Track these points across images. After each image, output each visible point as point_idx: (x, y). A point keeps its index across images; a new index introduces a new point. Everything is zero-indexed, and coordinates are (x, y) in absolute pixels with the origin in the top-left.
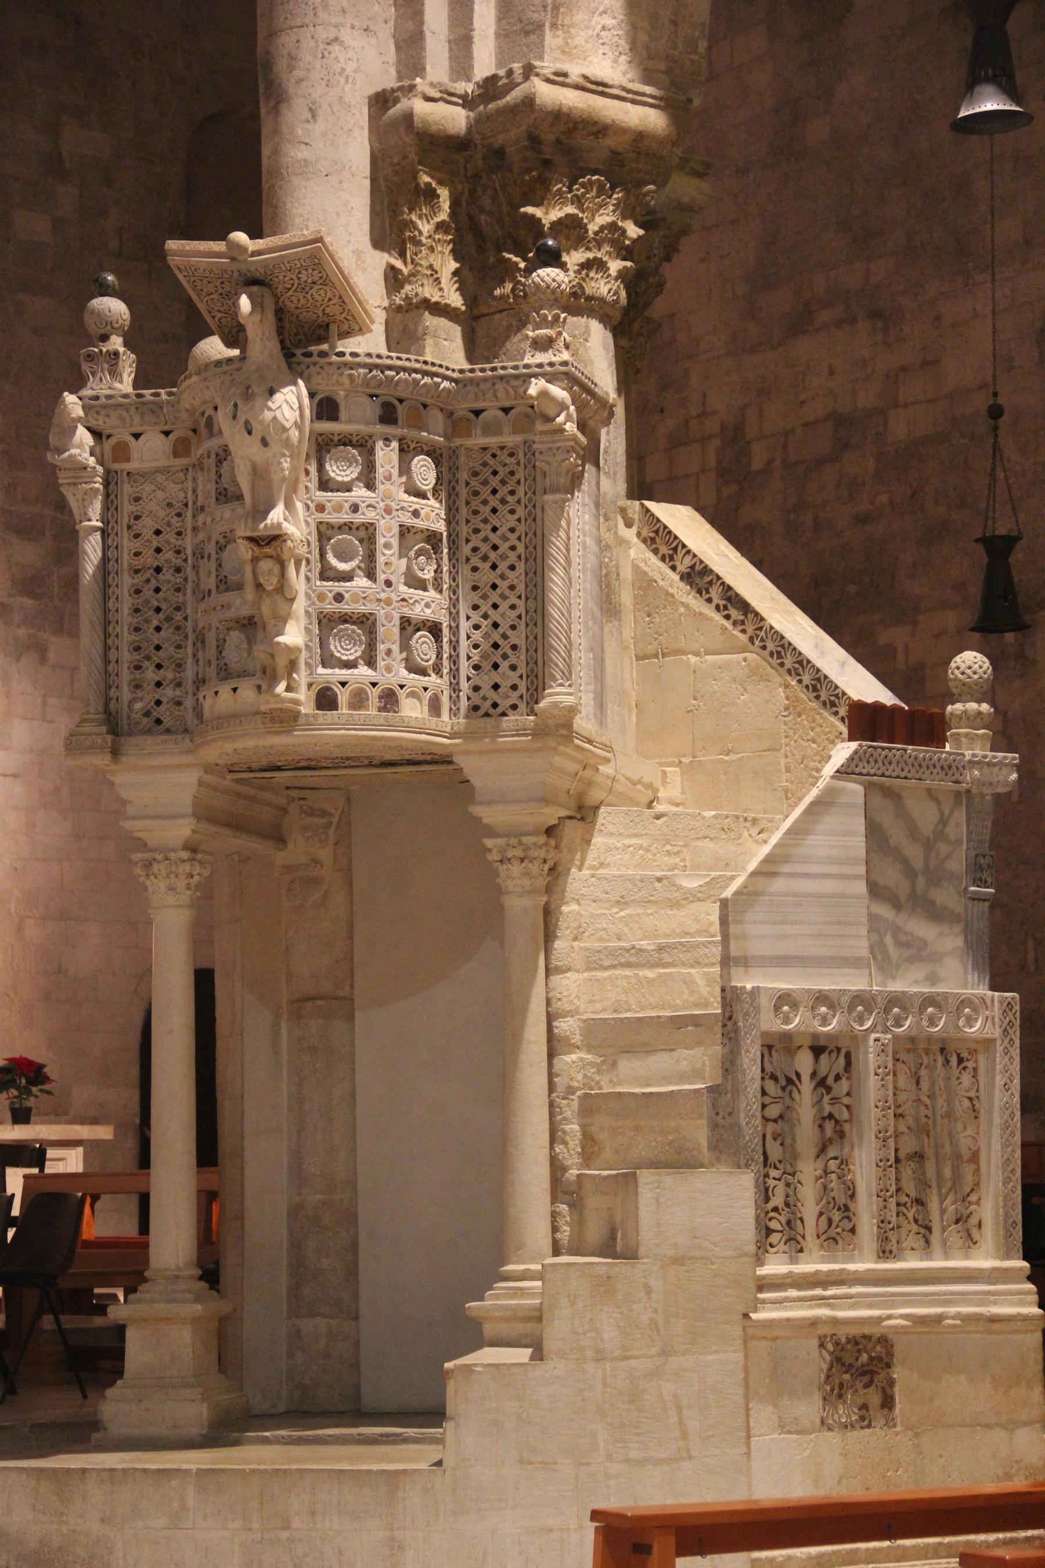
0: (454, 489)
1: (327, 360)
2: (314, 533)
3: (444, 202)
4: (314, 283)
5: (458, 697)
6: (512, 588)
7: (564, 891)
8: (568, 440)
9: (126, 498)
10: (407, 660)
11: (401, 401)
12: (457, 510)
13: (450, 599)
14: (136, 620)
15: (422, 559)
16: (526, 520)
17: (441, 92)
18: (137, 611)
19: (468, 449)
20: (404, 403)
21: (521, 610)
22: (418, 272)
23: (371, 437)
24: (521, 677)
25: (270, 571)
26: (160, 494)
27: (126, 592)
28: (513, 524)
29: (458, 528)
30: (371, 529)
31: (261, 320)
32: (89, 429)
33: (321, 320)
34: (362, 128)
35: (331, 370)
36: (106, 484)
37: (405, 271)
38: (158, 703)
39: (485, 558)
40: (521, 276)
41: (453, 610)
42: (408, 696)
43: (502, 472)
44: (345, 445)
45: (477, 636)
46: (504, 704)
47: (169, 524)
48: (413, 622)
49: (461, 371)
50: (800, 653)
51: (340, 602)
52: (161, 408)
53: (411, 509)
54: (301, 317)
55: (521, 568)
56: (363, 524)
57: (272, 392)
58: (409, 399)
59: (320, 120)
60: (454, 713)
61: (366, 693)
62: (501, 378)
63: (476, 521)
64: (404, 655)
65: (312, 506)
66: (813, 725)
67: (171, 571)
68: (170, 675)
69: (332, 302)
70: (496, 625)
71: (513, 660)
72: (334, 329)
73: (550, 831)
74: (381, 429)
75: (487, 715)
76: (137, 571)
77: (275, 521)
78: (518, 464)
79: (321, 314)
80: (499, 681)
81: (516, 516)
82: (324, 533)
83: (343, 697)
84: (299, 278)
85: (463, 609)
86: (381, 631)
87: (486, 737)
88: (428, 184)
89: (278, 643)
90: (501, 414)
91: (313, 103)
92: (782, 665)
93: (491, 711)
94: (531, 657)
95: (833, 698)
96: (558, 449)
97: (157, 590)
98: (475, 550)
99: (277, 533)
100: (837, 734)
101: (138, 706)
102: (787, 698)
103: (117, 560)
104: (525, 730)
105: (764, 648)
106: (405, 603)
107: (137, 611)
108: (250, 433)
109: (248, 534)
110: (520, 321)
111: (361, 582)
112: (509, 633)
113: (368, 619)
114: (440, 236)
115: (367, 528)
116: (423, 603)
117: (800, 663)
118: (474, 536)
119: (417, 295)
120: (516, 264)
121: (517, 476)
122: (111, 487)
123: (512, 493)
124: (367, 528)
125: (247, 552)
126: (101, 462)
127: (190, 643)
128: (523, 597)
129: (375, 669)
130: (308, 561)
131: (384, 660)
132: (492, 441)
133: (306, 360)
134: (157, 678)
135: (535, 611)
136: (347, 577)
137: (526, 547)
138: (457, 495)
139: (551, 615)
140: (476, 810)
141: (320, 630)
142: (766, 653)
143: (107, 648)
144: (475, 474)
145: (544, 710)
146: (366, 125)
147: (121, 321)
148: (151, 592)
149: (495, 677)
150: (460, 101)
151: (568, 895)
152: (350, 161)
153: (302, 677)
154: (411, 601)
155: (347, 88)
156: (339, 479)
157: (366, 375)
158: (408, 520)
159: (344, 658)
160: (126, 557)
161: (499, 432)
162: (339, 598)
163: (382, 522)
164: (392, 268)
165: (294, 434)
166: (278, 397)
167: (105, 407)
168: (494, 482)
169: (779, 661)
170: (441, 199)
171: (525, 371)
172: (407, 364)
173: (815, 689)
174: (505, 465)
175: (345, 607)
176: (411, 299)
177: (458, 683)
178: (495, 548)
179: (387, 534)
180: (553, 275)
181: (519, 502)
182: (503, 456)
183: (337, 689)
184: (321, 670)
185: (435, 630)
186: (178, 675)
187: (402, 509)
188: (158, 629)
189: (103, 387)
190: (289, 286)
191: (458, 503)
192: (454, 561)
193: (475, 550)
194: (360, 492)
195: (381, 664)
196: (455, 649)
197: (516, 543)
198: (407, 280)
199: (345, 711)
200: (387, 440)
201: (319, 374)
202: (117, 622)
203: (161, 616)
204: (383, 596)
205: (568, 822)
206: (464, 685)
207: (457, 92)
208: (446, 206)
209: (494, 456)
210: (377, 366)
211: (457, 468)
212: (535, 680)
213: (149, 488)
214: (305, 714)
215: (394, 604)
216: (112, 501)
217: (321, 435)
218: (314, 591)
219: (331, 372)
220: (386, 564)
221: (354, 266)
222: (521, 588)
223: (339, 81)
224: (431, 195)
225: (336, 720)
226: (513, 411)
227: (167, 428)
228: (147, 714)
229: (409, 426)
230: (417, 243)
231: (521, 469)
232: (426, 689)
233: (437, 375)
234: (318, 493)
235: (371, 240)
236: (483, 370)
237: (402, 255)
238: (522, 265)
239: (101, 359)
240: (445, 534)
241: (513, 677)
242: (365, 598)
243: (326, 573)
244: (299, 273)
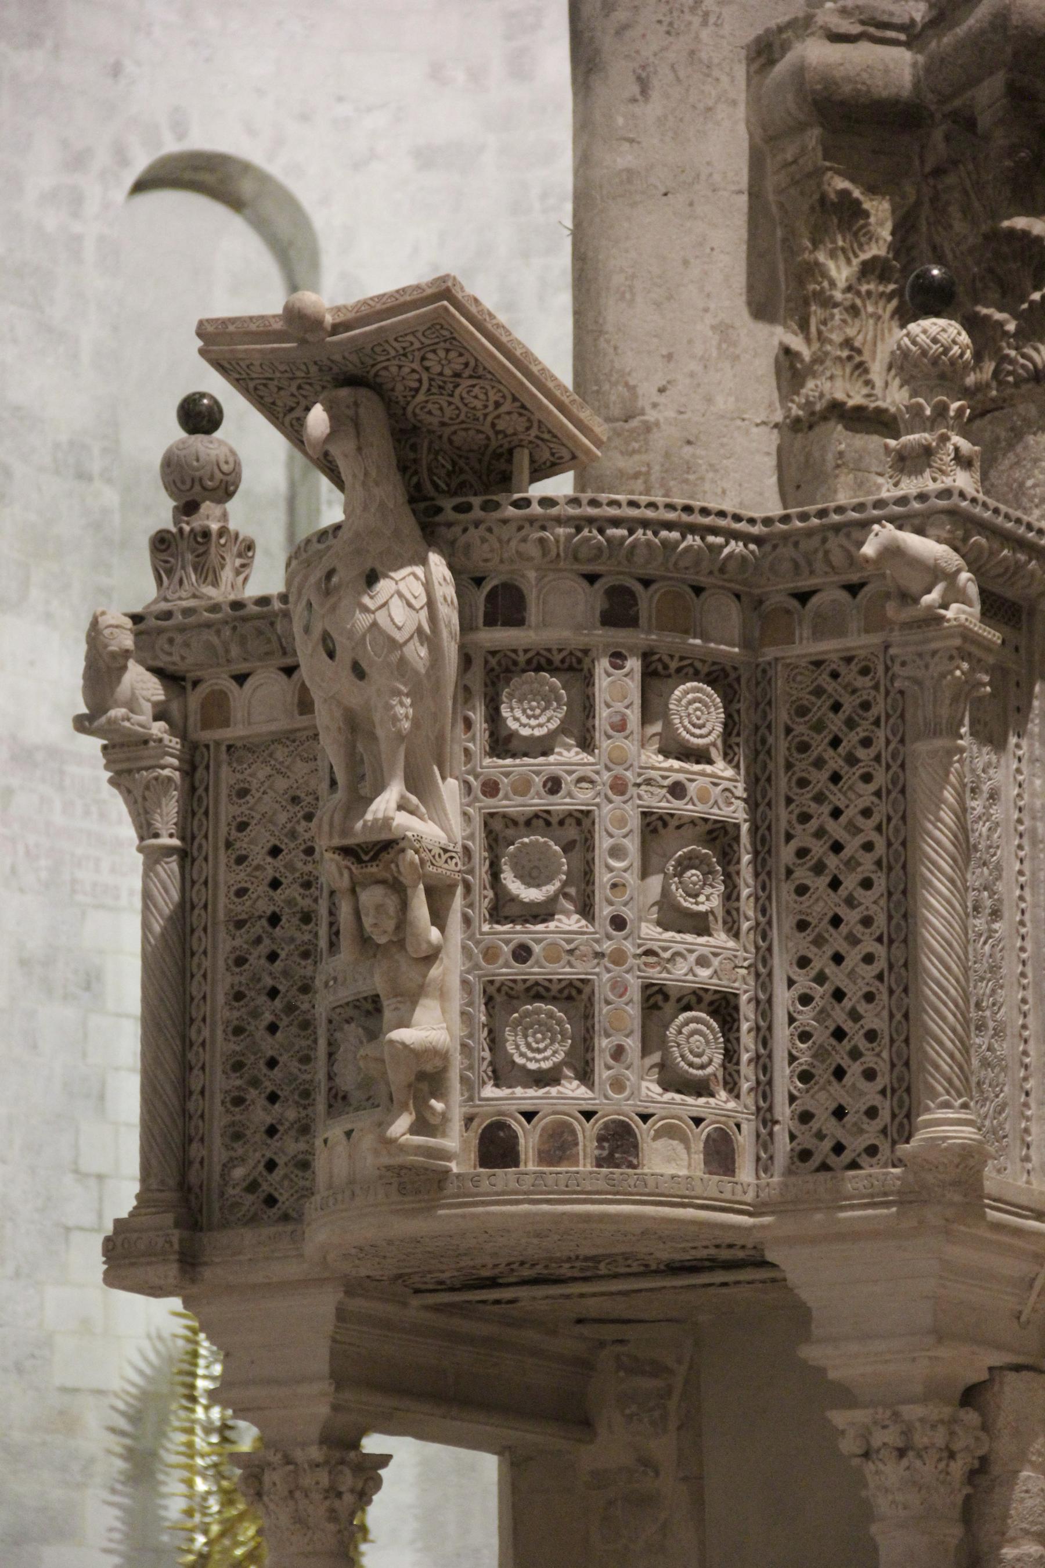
0: (764, 741)
1: (497, 515)
2: (480, 834)
3: (881, 224)
4: (457, 375)
5: (771, 1134)
7: (1006, 1516)
8: (951, 636)
9: (224, 791)
10: (662, 1066)
11: (647, 583)
12: (769, 780)
13: (757, 948)
14: (236, 1014)
15: (693, 875)
16: (889, 792)
17: (863, 23)
18: (239, 996)
19: (791, 667)
20: (654, 587)
21: (881, 964)
22: (827, 354)
23: (586, 652)
24: (883, 1092)
25: (379, 908)
26: (281, 784)
27: (221, 963)
28: (867, 801)
29: (771, 815)
30: (586, 823)
31: (359, 449)
32: (158, 672)
33: (494, 444)
34: (734, 103)
35: (505, 532)
36: (190, 768)
37: (806, 353)
38: (271, 1165)
39: (819, 868)
40: (1009, 346)
41: (762, 970)
42: (658, 1135)
44: (538, 669)
45: (806, 1016)
46: (855, 1145)
47: (293, 835)
48: (674, 995)
49: (767, 521)
51: (524, 962)
52: (272, 624)
53: (666, 783)
54: (457, 440)
55: (880, 883)
56: (570, 814)
57: (372, 579)
58: (664, 578)
59: (655, 94)
60: (763, 1165)
61: (573, 1132)
62: (837, 528)
63: (804, 799)
64: (656, 1057)
65: (476, 784)
67: (295, 921)
68: (291, 1114)
69: (503, 409)
70: (839, 995)
71: (869, 1060)
72: (522, 461)
73: (971, 1396)
74: (602, 636)
75: (824, 1167)
76: (240, 924)
77: (380, 815)
78: (876, 687)
79: (491, 433)
80: (846, 1100)
81: (872, 787)
82: (498, 832)
83: (528, 1140)
84: (427, 369)
85: (781, 966)
86: (602, 1012)
87: (818, 1209)
88: (845, 194)
89: (391, 1042)
90: (844, 596)
91: (643, 67)
93: (833, 1160)
94: (899, 1055)
96: (934, 653)
97: (273, 957)
99: (384, 836)
101: (238, 1173)
103: (205, 907)
104: (885, 1194)
106: (652, 959)
107: (239, 996)
108: (331, 655)
109: (337, 842)
110: (1012, 429)
111: (569, 922)
112: (862, 1008)
113: (580, 991)
114: (872, 287)
115: (579, 823)
116: (692, 958)
118: (799, 827)
119: (822, 396)
120: (1001, 324)
121: (874, 711)
122: (200, 773)
123: (866, 743)
124: (579, 823)
125: (341, 874)
126: (174, 729)
128: (885, 939)
129: (591, 1086)
130: (468, 888)
131: (609, 1068)
132: (828, 647)
133: (461, 517)
134: (269, 1120)
136: (542, 913)
137: (889, 844)
138: (769, 752)
139: (926, 970)
140: (811, 1353)
141: (489, 1015)
143: (186, 1068)
144: (802, 711)
146: (742, 97)
147: (219, 476)
148: (263, 961)
149: (839, 1093)
150: (903, 37)
151: (1015, 1524)
152: (708, 163)
153: (450, 1106)
154: (667, 955)
155: (705, 34)
156: (525, 732)
157: (569, 538)
158: (660, 802)
159: (532, 1066)
160: (222, 901)
161: (840, 631)
162: (522, 953)
163: (607, 808)
164: (787, 351)
165: (418, 654)
166: (384, 587)
167: (182, 629)
168: (836, 723)
170: (872, 220)
171: (876, 512)
172: (650, 514)
174: (854, 691)
175: (534, 971)
176: (813, 404)
177: (770, 1109)
178: (837, 847)
179: (617, 830)
180: (933, 331)
181: (877, 758)
182: (850, 674)
183: (518, 1126)
184: (489, 1091)
185: (723, 1009)
186: (303, 1113)
187: (648, 782)
188: (273, 1028)
189: (184, 594)
190: (415, 385)
191: (771, 766)
192: (763, 876)
193: (802, 853)
194: (568, 756)
195: (602, 1074)
196: (765, 1044)
197: (874, 836)
198: (810, 371)
199: (531, 1167)
200: (618, 658)
201: (484, 540)
202: (204, 1020)
203: (278, 1003)
204: (607, 946)
205: (1011, 1377)
206: (783, 1111)
207: (896, 20)
208: (885, 233)
209: (835, 675)
210: (591, 521)
211: (769, 703)
213: (263, 772)
214: (458, 1176)
215: (631, 961)
216: (200, 798)
217: (493, 653)
218: (477, 943)
219: (505, 538)
220: (614, 886)
221: (715, 353)
222: (881, 921)
223: (690, 23)
224: (849, 215)
225: (513, 1185)
226: (866, 589)
228: (253, 1187)
229: (661, 628)
230: (828, 303)
231: (880, 698)
232: (698, 1121)
233: (714, 531)
234: (487, 761)
235: (749, 304)
236: (804, 517)
237: (804, 326)
238: (1011, 327)
239: (183, 545)
240: (745, 827)
242: (571, 952)
243: (504, 908)
244: (423, 359)
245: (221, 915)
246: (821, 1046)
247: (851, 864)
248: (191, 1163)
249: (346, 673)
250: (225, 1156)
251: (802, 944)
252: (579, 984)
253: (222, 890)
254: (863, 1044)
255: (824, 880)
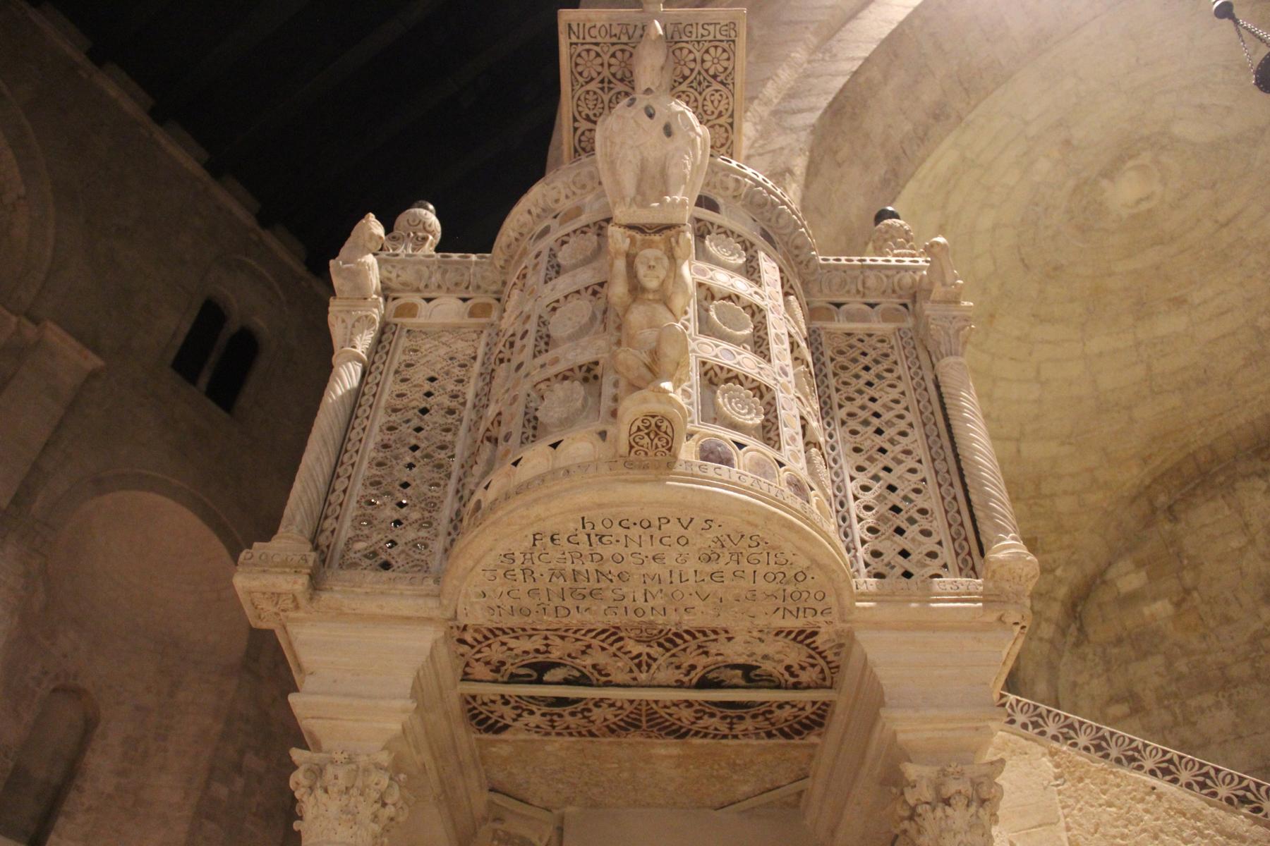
5: (855, 556)
6: (907, 452)
28: (896, 396)
38: (394, 543)
39: (866, 423)
43: (873, 354)
50: (1066, 718)
55: (916, 434)
62: (870, 267)
66: (1105, 787)
68: (415, 515)
76: (395, 410)
80: (908, 546)
87: (911, 601)
92: (1043, 733)
95: (1130, 753)
98: (851, 415)
100: (1149, 789)
102: (1057, 766)
104: (970, 594)
105: (1012, 722)
107: (386, 446)
108: (651, 116)
112: (913, 496)
117: (1071, 726)
127: (453, 480)
132: (858, 327)
135: (948, 472)
142: (1017, 726)
143: (334, 475)
144: (841, 353)
145: (1002, 564)
149: (902, 542)
157: (751, 187)
160: (385, 397)
161: (864, 319)
169: (1037, 731)
173: (1098, 748)
178: (877, 415)
186: (427, 514)
188: (411, 466)
196: (842, 504)
209: (862, 341)
212: (964, 543)
222: (921, 451)
225: (735, 478)
227: (466, 296)
241: (929, 544)
245: (383, 403)
246: (882, 515)
247: (890, 424)
248: (322, 531)
249: (660, 128)
250: (351, 534)
251: (860, 459)
252: (764, 389)
253: (387, 391)
254: (917, 516)
255: (871, 429)
